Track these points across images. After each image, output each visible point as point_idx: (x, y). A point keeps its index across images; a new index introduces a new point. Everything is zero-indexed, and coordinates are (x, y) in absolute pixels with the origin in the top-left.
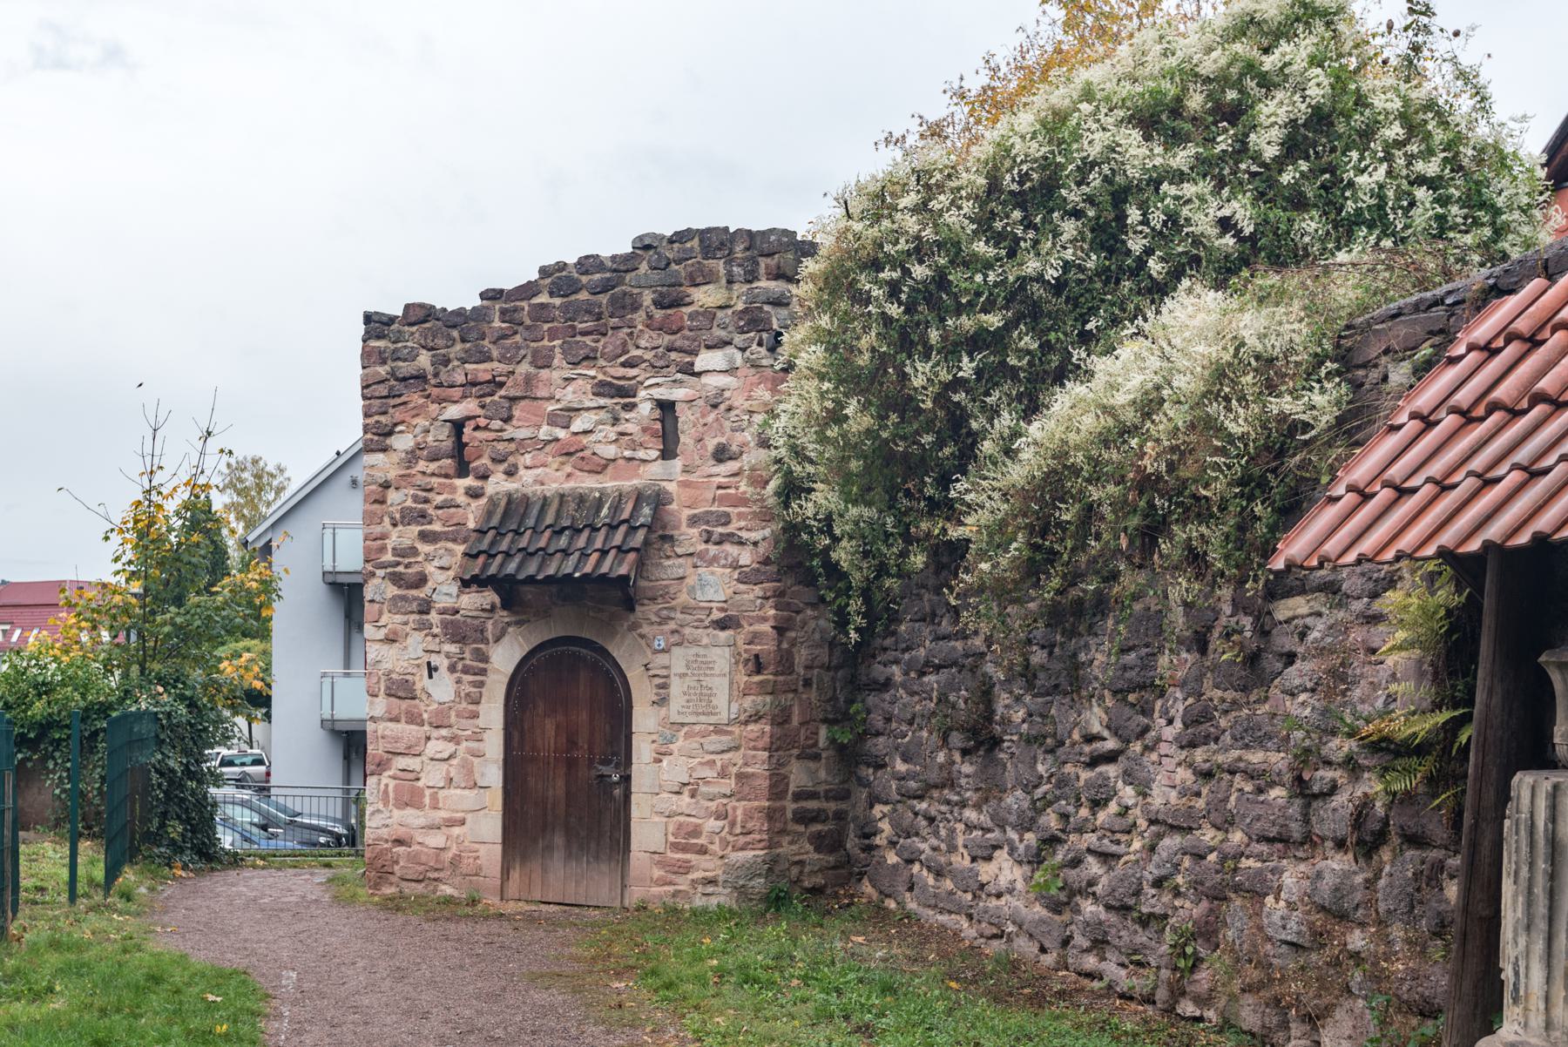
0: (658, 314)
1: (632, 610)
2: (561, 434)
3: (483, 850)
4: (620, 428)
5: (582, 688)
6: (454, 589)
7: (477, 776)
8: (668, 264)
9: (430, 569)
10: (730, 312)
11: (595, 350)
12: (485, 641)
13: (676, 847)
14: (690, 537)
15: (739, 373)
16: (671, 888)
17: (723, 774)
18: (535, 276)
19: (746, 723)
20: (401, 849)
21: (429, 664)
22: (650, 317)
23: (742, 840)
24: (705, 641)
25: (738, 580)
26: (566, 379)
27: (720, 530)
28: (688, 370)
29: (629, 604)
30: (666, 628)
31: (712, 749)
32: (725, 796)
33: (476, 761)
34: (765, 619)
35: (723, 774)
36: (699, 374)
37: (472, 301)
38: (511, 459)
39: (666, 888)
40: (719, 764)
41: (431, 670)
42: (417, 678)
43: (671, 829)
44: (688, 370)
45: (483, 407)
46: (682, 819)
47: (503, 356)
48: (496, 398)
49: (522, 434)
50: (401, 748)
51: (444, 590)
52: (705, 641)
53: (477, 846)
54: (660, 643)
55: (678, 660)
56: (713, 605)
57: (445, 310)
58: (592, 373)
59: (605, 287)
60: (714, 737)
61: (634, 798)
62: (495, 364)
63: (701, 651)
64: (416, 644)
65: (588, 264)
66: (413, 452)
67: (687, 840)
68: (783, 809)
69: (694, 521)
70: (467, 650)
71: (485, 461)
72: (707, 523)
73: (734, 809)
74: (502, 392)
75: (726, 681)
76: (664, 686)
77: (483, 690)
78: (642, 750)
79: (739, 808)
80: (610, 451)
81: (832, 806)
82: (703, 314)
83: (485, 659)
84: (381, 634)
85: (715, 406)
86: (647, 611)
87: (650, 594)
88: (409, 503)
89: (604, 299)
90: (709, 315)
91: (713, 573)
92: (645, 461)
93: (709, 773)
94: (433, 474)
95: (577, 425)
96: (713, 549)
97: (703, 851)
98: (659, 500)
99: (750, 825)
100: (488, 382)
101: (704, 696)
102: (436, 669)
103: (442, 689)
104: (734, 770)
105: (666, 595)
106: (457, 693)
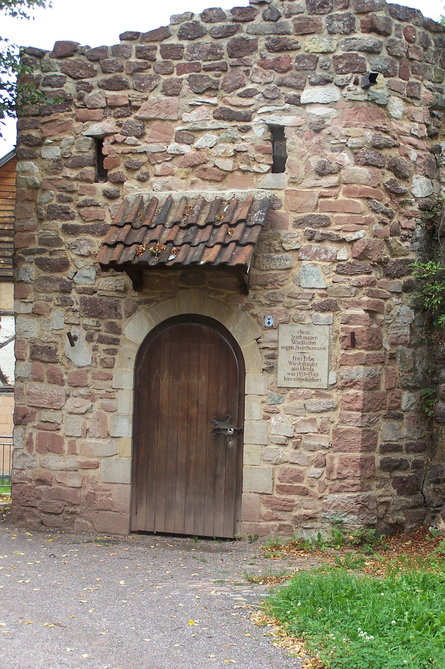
0: (271, 57)
1: (246, 293)
2: (185, 149)
3: (115, 490)
4: (235, 146)
6: (92, 274)
7: (109, 428)
8: (279, 17)
9: (71, 255)
10: (331, 57)
11: (217, 83)
12: (118, 316)
13: (281, 489)
14: (294, 236)
15: (338, 105)
16: (277, 523)
17: (322, 430)
18: (166, 23)
19: (343, 388)
20: (43, 487)
21: (69, 334)
22: (263, 58)
23: (338, 484)
24: (308, 320)
25: (336, 272)
26: (192, 105)
27: (321, 231)
28: (295, 101)
29: (244, 288)
30: (275, 309)
31: (313, 409)
32: (324, 448)
33: (109, 415)
34: (358, 304)
36: (305, 105)
37: (112, 40)
38: (144, 169)
39: (272, 523)
40: (319, 421)
41: (72, 340)
42: (59, 346)
43: (277, 474)
44: (295, 101)
45: (120, 125)
46: (287, 466)
47: (139, 86)
48: (131, 119)
49: (153, 147)
50: (44, 402)
51: (84, 274)
52: (308, 320)
53: (110, 486)
55: (285, 336)
56: (314, 291)
57: (88, 47)
58: (214, 101)
59: (227, 33)
61: (245, 448)
62: (131, 92)
63: (305, 329)
64: (58, 318)
65: (210, 15)
66: (58, 161)
68: (373, 459)
69: (299, 223)
70: (102, 323)
71: (121, 169)
72: (311, 225)
73: (332, 458)
74: (137, 114)
75: (326, 354)
76: (273, 357)
77: (116, 357)
78: (253, 409)
79: (336, 459)
80: (228, 165)
81: (412, 457)
82: (309, 57)
83: (116, 330)
84: (29, 308)
85: (318, 131)
86: (262, 296)
87: (261, 281)
88: (54, 202)
89: (225, 43)
90: (313, 58)
93: (310, 429)
94: (76, 179)
95: (201, 141)
96: (315, 246)
97: (304, 493)
98: (270, 206)
99: (345, 472)
100: (126, 106)
102: (76, 338)
103: (82, 355)
104: (332, 427)
106: (94, 359)
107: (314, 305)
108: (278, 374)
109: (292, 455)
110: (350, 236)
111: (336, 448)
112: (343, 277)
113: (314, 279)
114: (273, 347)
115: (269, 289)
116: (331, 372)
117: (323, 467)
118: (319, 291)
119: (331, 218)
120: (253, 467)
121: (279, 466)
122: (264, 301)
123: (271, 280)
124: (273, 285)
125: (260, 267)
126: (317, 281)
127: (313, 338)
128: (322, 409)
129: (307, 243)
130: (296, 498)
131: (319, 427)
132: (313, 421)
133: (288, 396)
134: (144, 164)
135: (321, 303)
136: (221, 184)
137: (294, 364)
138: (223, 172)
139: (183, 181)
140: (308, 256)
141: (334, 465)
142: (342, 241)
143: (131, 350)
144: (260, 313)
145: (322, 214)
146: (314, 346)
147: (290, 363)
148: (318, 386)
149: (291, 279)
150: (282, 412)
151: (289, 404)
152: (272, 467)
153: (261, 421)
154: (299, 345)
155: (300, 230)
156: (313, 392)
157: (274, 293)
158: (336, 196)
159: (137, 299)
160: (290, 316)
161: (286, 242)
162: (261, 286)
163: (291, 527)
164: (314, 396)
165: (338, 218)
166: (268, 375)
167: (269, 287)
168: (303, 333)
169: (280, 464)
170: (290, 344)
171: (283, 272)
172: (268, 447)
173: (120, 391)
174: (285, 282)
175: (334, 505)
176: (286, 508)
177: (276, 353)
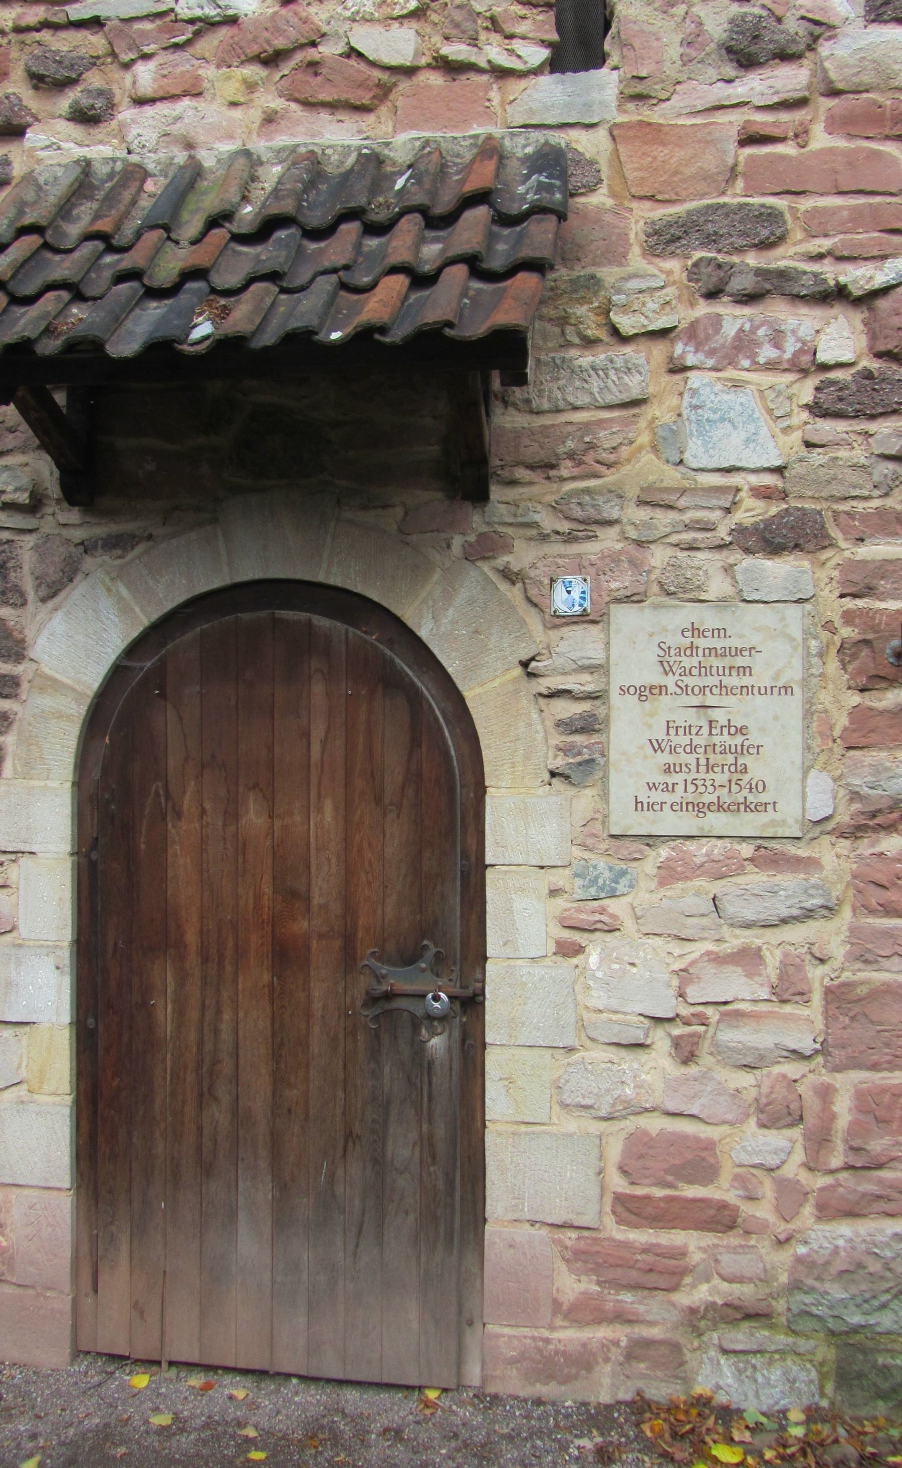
1: (480, 496)
5: (318, 732)
13: (630, 1209)
14: (648, 287)
16: (621, 1333)
17: (789, 990)
25: (817, 410)
27: (752, 260)
30: (590, 549)
35: (789, 990)
38: (94, 80)
39: (603, 1333)
43: (615, 1151)
52: (718, 586)
54: (567, 597)
55: (635, 644)
56: (736, 480)
60: (756, 879)
61: (494, 1062)
63: (708, 618)
67: (667, 1184)
69: (664, 240)
72: (711, 240)
73: (826, 1093)
75: (794, 705)
76: (587, 726)
78: (518, 919)
87: (533, 451)
91: (736, 385)
92: (502, 73)
93: (735, 986)
96: (733, 318)
97: (721, 1219)
101: (720, 763)
104: (817, 975)
105: (587, 457)
107: (740, 531)
108: (613, 789)
110: (860, 277)
111: (839, 1055)
112: (841, 426)
113: (737, 437)
114: (589, 688)
115: (563, 480)
116: (813, 773)
117: (790, 1125)
119: (788, 216)
120: (523, 1128)
121: (623, 1124)
122: (548, 522)
123: (570, 444)
124: (580, 463)
125: (528, 401)
126: (748, 441)
127: (739, 652)
128: (785, 913)
129: (703, 309)
130: (693, 1243)
131: (774, 980)
132: (748, 958)
133: (649, 866)
134: (94, 62)
135: (768, 523)
136: (371, 118)
137: (673, 750)
138: (377, 74)
139: (237, 113)
140: (711, 353)
141: (833, 1117)
142: (836, 295)
143: (60, 716)
144: (533, 566)
145: (756, 200)
146: (746, 681)
147: (657, 747)
148: (765, 826)
149: (644, 439)
150: (629, 925)
151: (656, 897)
152: (596, 1127)
153: (548, 962)
154: (690, 681)
155: (673, 265)
156: (747, 850)
157: (587, 491)
158: (801, 135)
159: (79, 534)
160: (649, 572)
161: (625, 308)
162: (531, 467)
163: (676, 1348)
164: (750, 867)
165: (814, 212)
166: (572, 791)
167: (565, 473)
168: (701, 633)
169: (625, 1117)
170: (655, 677)
171: (616, 414)
172: (577, 1056)
173: (24, 860)
174: (625, 451)
175: (840, 1265)
176: (653, 1279)
177: (601, 711)
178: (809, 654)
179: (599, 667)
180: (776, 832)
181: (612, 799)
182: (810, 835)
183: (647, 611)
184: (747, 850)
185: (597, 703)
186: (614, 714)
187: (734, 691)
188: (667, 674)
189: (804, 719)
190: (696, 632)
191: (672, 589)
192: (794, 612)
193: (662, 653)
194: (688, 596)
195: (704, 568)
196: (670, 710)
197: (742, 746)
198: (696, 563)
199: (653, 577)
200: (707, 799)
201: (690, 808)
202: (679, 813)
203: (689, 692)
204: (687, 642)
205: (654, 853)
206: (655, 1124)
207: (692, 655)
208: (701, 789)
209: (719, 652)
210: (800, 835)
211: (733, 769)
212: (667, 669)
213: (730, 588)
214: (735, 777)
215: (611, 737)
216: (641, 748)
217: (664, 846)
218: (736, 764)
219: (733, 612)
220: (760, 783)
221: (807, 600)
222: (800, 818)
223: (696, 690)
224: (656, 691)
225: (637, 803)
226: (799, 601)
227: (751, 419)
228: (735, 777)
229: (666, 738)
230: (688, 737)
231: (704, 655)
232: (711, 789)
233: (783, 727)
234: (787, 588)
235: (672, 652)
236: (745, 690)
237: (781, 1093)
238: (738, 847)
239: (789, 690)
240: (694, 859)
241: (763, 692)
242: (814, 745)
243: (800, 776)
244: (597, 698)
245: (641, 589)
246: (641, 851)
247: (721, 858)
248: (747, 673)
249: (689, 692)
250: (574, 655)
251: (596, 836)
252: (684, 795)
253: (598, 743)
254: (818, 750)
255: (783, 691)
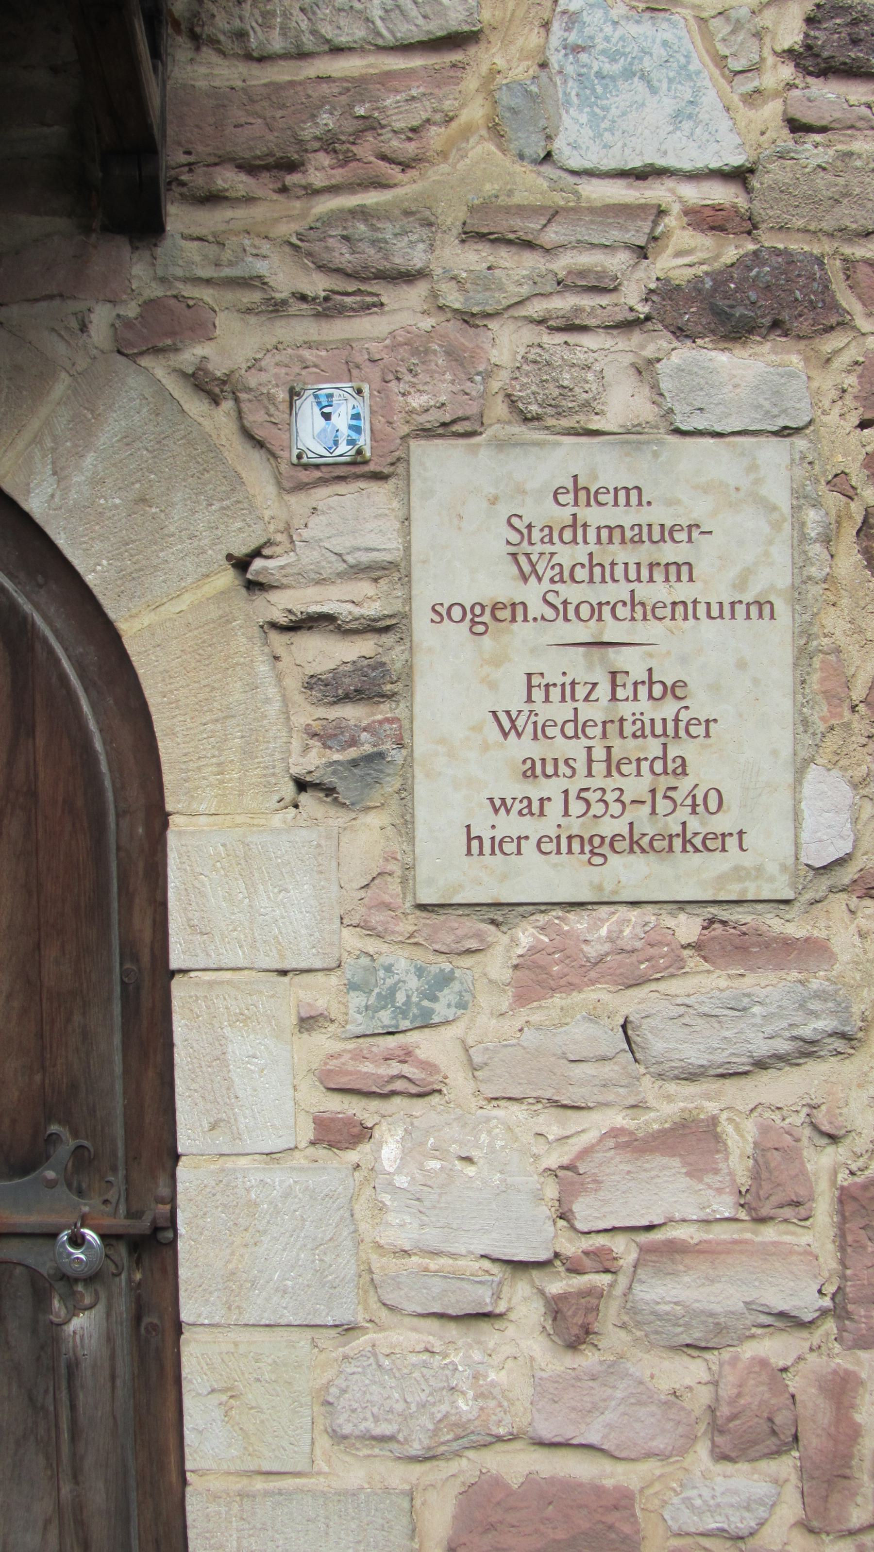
17: (768, 1198)
25: (811, 61)
35: (768, 1198)
52: (623, 402)
54: (321, 428)
55: (459, 523)
56: (656, 192)
60: (706, 983)
61: (196, 1357)
63: (607, 467)
75: (776, 639)
76: (367, 686)
78: (238, 1078)
87: (254, 136)
93: (669, 1195)
101: (630, 756)
104: (822, 1164)
105: (361, 146)
107: (665, 293)
108: (421, 813)
109: (545, 1390)
113: (658, 109)
114: (372, 609)
115: (314, 192)
116: (813, 773)
117: (776, 1453)
118: (691, 193)
120: (259, 1484)
121: (454, 1466)
122: (285, 276)
123: (327, 120)
124: (347, 159)
125: (241, 35)
126: (678, 117)
127: (668, 533)
128: (763, 1048)
131: (744, 1180)
132: (692, 1140)
133: (497, 965)
135: (721, 278)
137: (540, 732)
144: (255, 365)
146: (683, 591)
147: (508, 726)
148: (722, 879)
149: (475, 112)
150: (459, 1081)
151: (510, 1026)
152: (400, 1476)
153: (299, 1159)
154: (572, 593)
156: (687, 927)
157: (362, 213)
160: (487, 376)
162: (250, 168)
164: (693, 961)
166: (337, 819)
167: (317, 179)
168: (593, 498)
169: (458, 1454)
170: (501, 585)
171: (417, 62)
172: (361, 1342)
174: (436, 136)
177: (396, 657)
178: (803, 538)
179: (392, 566)
180: (745, 891)
181: (421, 831)
182: (808, 896)
183: (484, 454)
184: (687, 927)
185: (388, 639)
186: (421, 661)
187: (659, 613)
188: (525, 579)
189: (795, 665)
190: (582, 495)
191: (534, 408)
192: (773, 455)
193: (515, 538)
194: (565, 423)
195: (597, 367)
196: (533, 651)
197: (677, 720)
198: (580, 356)
199: (495, 385)
200: (608, 827)
201: (576, 846)
202: (553, 858)
203: (571, 614)
204: (565, 515)
205: (505, 939)
206: (516, 1465)
207: (575, 541)
208: (597, 809)
209: (629, 534)
210: (789, 894)
211: (658, 767)
212: (527, 568)
213: (649, 406)
214: (664, 783)
215: (417, 709)
216: (477, 728)
217: (524, 924)
218: (665, 758)
219: (656, 455)
220: (713, 795)
221: (797, 430)
222: (791, 861)
223: (585, 611)
224: (506, 614)
225: (469, 839)
226: (785, 432)
227: (685, 74)
228: (664, 783)
229: (526, 708)
230: (570, 705)
231: (599, 541)
232: (615, 809)
233: (756, 681)
234: (760, 406)
235: (536, 535)
236: (680, 609)
237: (757, 1394)
238: (670, 922)
239: (767, 609)
240: (585, 948)
241: (715, 612)
242: (815, 718)
243: (789, 778)
244: (387, 629)
245: (472, 409)
246: (479, 936)
247: (638, 944)
248: (685, 577)
249: (571, 614)
250: (341, 544)
251: (389, 907)
252: (563, 821)
253: (387, 720)
254: (822, 727)
255: (754, 610)
